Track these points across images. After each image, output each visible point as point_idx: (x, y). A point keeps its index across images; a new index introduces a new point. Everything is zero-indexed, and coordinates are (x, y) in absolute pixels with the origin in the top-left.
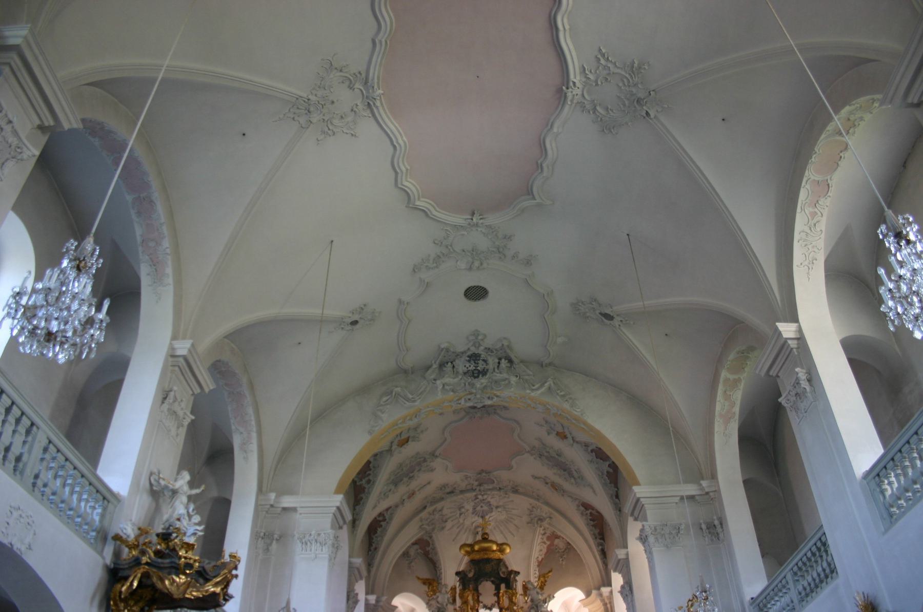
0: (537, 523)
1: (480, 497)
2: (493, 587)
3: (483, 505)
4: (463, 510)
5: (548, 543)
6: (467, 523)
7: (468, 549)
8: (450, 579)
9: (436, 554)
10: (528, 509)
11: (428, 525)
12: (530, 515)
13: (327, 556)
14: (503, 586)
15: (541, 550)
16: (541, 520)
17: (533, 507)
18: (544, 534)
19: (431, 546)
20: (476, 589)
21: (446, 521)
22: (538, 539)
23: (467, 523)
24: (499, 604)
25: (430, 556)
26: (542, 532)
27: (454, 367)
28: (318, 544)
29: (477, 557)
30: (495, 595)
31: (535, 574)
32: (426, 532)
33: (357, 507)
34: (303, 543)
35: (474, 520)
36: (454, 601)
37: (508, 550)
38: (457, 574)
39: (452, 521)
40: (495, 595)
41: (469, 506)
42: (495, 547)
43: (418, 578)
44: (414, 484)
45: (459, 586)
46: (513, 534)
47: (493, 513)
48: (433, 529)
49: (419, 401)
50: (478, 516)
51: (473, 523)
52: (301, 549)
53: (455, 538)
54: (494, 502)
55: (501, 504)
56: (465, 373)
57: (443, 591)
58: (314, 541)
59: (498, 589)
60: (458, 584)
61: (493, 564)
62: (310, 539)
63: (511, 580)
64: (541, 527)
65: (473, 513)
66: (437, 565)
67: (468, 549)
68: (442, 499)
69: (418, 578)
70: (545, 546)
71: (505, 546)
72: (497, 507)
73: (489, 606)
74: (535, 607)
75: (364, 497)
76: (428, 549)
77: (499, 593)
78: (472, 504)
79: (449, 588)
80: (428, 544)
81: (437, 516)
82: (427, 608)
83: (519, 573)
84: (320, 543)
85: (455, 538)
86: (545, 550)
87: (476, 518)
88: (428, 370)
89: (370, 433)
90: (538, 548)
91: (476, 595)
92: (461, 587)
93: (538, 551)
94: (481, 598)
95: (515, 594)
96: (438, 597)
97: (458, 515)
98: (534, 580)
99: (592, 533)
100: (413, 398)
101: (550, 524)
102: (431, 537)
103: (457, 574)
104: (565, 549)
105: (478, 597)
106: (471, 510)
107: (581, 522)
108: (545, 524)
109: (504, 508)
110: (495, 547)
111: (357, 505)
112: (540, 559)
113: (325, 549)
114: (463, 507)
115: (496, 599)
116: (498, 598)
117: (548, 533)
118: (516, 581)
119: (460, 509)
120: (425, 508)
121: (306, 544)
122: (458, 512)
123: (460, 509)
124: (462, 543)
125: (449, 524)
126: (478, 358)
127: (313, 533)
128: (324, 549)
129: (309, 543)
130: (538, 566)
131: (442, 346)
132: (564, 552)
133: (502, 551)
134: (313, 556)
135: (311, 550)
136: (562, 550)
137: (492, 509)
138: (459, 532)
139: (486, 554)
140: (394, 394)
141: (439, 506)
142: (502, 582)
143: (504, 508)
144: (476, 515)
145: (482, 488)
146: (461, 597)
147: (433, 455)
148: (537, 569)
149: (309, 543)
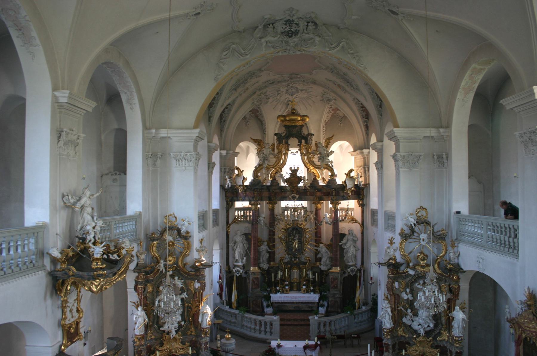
0: (327, 102)
1: (291, 85)
2: (297, 141)
3: (293, 89)
4: (280, 92)
5: (333, 112)
6: (282, 99)
7: (283, 119)
8: (271, 139)
9: (263, 117)
10: (322, 93)
11: (257, 102)
12: (323, 96)
13: (193, 168)
14: (303, 141)
15: (328, 116)
16: (329, 100)
17: (325, 92)
18: (331, 108)
19: (259, 112)
21: (269, 98)
22: (327, 110)
23: (282, 99)
25: (259, 117)
26: (330, 107)
27: (274, 27)
28: (186, 161)
29: (288, 124)
30: (298, 145)
31: (324, 130)
32: (256, 106)
33: (211, 109)
34: (176, 160)
35: (286, 97)
36: (273, 150)
37: (308, 120)
38: (276, 134)
39: (273, 98)
40: (298, 145)
41: (284, 90)
42: (299, 119)
43: (252, 139)
44: (247, 85)
45: (277, 142)
46: (311, 106)
47: (299, 94)
48: (261, 104)
49: (249, 55)
51: (286, 98)
52: (176, 164)
53: (274, 108)
54: (300, 88)
55: (304, 88)
56: (282, 33)
57: (267, 147)
58: (183, 159)
59: (300, 142)
60: (276, 141)
62: (181, 157)
64: (329, 104)
65: (286, 93)
66: (263, 123)
67: (283, 119)
68: (266, 87)
69: (252, 139)
70: (331, 114)
71: (305, 118)
72: (301, 90)
75: (215, 103)
76: (257, 114)
78: (286, 88)
79: (271, 145)
80: (258, 111)
81: (263, 96)
82: (257, 155)
83: (313, 135)
84: (188, 160)
85: (274, 108)
86: (330, 116)
87: (288, 96)
88: (255, 30)
89: (216, 79)
90: (326, 115)
92: (278, 143)
93: (326, 116)
95: (310, 147)
96: (264, 150)
97: (276, 95)
98: (323, 142)
99: (361, 114)
100: (244, 53)
101: (334, 103)
102: (259, 108)
103: (276, 134)
104: (343, 117)
105: (288, 147)
106: (285, 91)
107: (355, 108)
108: (332, 103)
109: (306, 91)
111: (211, 108)
112: (327, 120)
113: (191, 164)
114: (280, 90)
117: (333, 107)
118: (312, 140)
119: (278, 91)
120: (255, 93)
121: (179, 161)
122: (277, 93)
123: (278, 91)
124: (280, 113)
125: (270, 100)
126: (292, 23)
127: (182, 154)
128: (190, 164)
129: (180, 161)
130: (326, 125)
131: (265, 17)
133: (303, 120)
134: (184, 168)
135: (182, 165)
137: (298, 91)
138: (277, 104)
139: (294, 123)
140: (231, 49)
141: (264, 91)
143: (306, 91)
145: (292, 80)
146: (278, 148)
147: (260, 70)
148: (325, 127)
149: (180, 161)
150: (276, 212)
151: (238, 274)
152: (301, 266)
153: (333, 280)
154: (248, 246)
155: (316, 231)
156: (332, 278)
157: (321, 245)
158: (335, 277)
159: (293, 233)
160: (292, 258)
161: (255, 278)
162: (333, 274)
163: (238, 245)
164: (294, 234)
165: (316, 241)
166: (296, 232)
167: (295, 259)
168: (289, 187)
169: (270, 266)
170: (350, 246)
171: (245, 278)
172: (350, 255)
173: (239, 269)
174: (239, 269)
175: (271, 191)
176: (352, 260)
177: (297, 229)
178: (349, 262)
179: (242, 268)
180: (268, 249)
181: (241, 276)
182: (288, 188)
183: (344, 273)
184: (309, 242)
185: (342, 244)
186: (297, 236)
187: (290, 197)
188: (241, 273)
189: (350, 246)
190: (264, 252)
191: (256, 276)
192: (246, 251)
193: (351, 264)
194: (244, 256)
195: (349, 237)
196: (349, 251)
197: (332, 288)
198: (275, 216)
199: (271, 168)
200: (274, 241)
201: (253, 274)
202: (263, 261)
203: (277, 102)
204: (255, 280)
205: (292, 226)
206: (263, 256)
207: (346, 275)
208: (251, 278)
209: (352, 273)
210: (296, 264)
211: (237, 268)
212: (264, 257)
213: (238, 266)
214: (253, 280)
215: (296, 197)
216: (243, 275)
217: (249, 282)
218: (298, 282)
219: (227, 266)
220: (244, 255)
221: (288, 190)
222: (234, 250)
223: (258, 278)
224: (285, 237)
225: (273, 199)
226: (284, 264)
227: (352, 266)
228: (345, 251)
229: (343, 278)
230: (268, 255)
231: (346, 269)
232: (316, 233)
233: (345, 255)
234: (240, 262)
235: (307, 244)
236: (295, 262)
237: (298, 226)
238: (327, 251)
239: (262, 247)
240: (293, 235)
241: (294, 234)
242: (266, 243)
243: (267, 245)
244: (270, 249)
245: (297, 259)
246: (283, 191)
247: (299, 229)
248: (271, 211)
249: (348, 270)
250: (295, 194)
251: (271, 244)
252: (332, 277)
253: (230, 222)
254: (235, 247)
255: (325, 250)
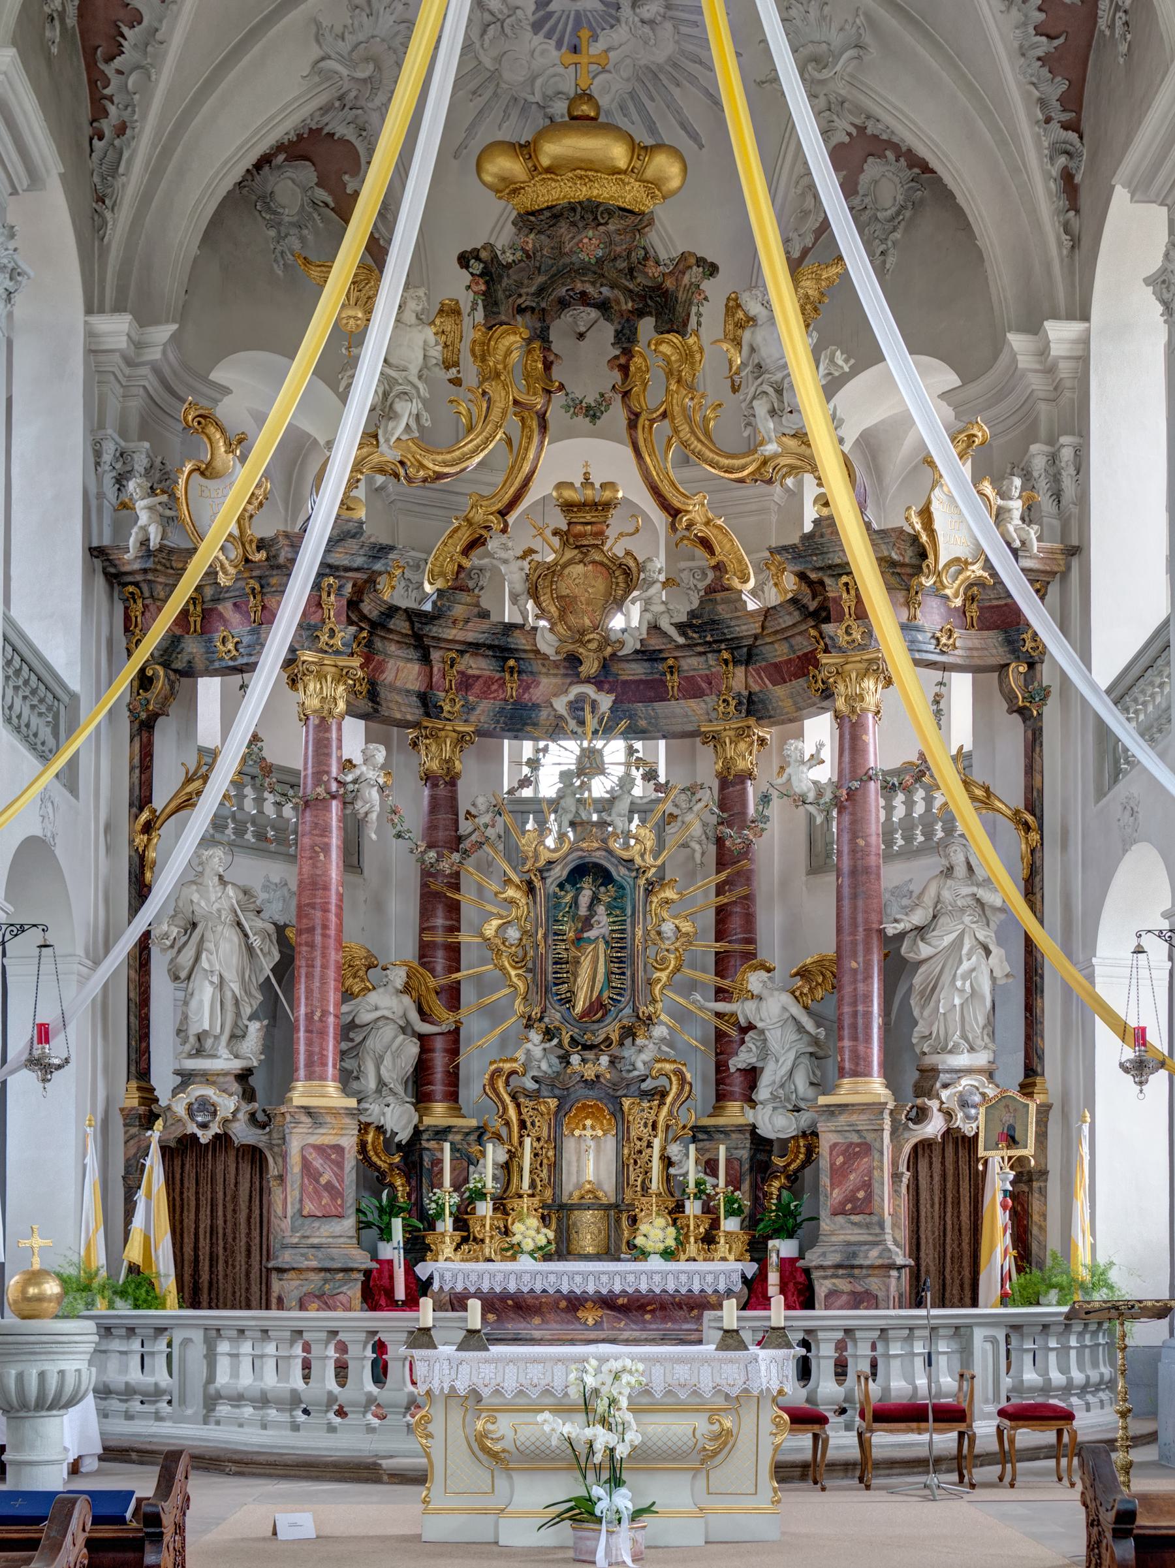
14: (646, 326)
20: (542, 336)
24: (626, 395)
50: (559, 45)
59: (626, 339)
61: (611, 227)
63: (681, 296)
73: (590, 400)
74: (770, 390)
77: (628, 353)
91: (537, 354)
94: (557, 374)
105: (548, 366)
110: (618, 154)
115: (617, 376)
116: (625, 369)
132: (893, 218)
136: (889, 213)
142: (641, 314)
144: (549, 36)
146: (482, 354)
150: (470, 794)
151: (204, 1126)
152: (626, 1103)
153: (840, 1160)
154: (277, 957)
155: (723, 900)
156: (833, 1147)
157: (755, 981)
158: (855, 1139)
159: (575, 901)
160: (565, 1059)
161: (320, 1149)
162: (843, 1119)
163: (209, 935)
164: (583, 911)
165: (722, 964)
166: (595, 900)
167: (590, 1055)
168: (549, 636)
169: (427, 1121)
170: (958, 942)
171: (255, 1156)
172: (950, 1000)
173: (210, 1092)
174: (210, 1092)
175: (435, 655)
176: (964, 1037)
177: (603, 876)
178: (944, 1050)
179: (235, 1087)
180: (414, 1016)
181: (222, 1140)
182: (547, 643)
183: (921, 1115)
184: (678, 969)
185: (901, 936)
186: (603, 923)
187: (560, 705)
188: (226, 1121)
189: (958, 942)
190: (388, 1032)
191: (325, 1137)
192: (266, 986)
193: (962, 1060)
194: (250, 1019)
195: (946, 895)
196: (946, 978)
197: (839, 1211)
198: (465, 827)
199: (434, 462)
200: (454, 963)
201: (305, 1119)
202: (381, 1083)
203: (480, 102)
204: (318, 1162)
205: (571, 850)
206: (381, 1058)
207: (934, 1127)
208: (295, 1146)
209: (968, 1117)
210: (590, 1084)
211: (197, 1091)
212: (387, 1061)
213: (206, 1077)
214: (306, 1165)
215: (594, 705)
216: (243, 1133)
217: (281, 1178)
218: (605, 1201)
219: (134, 1084)
220: (247, 1011)
221: (546, 657)
222: (182, 978)
223: (339, 1149)
224: (525, 932)
225: (447, 708)
226: (514, 1098)
227: (969, 1071)
228: (917, 980)
229: (907, 1149)
230: (413, 1049)
231: (929, 1093)
232: (722, 914)
233: (916, 1013)
234: (223, 1051)
235: (663, 976)
236: (589, 1072)
237: (610, 852)
238: (796, 1010)
239: (373, 998)
240: (575, 917)
241: (583, 911)
242: (398, 977)
243: (407, 989)
244: (424, 1015)
245: (604, 1060)
246: (511, 663)
247: (619, 873)
248: (435, 786)
249: (944, 1094)
250: (590, 690)
251: (432, 983)
252: (833, 1138)
253: (160, 801)
254: (188, 954)
255: (785, 1009)
